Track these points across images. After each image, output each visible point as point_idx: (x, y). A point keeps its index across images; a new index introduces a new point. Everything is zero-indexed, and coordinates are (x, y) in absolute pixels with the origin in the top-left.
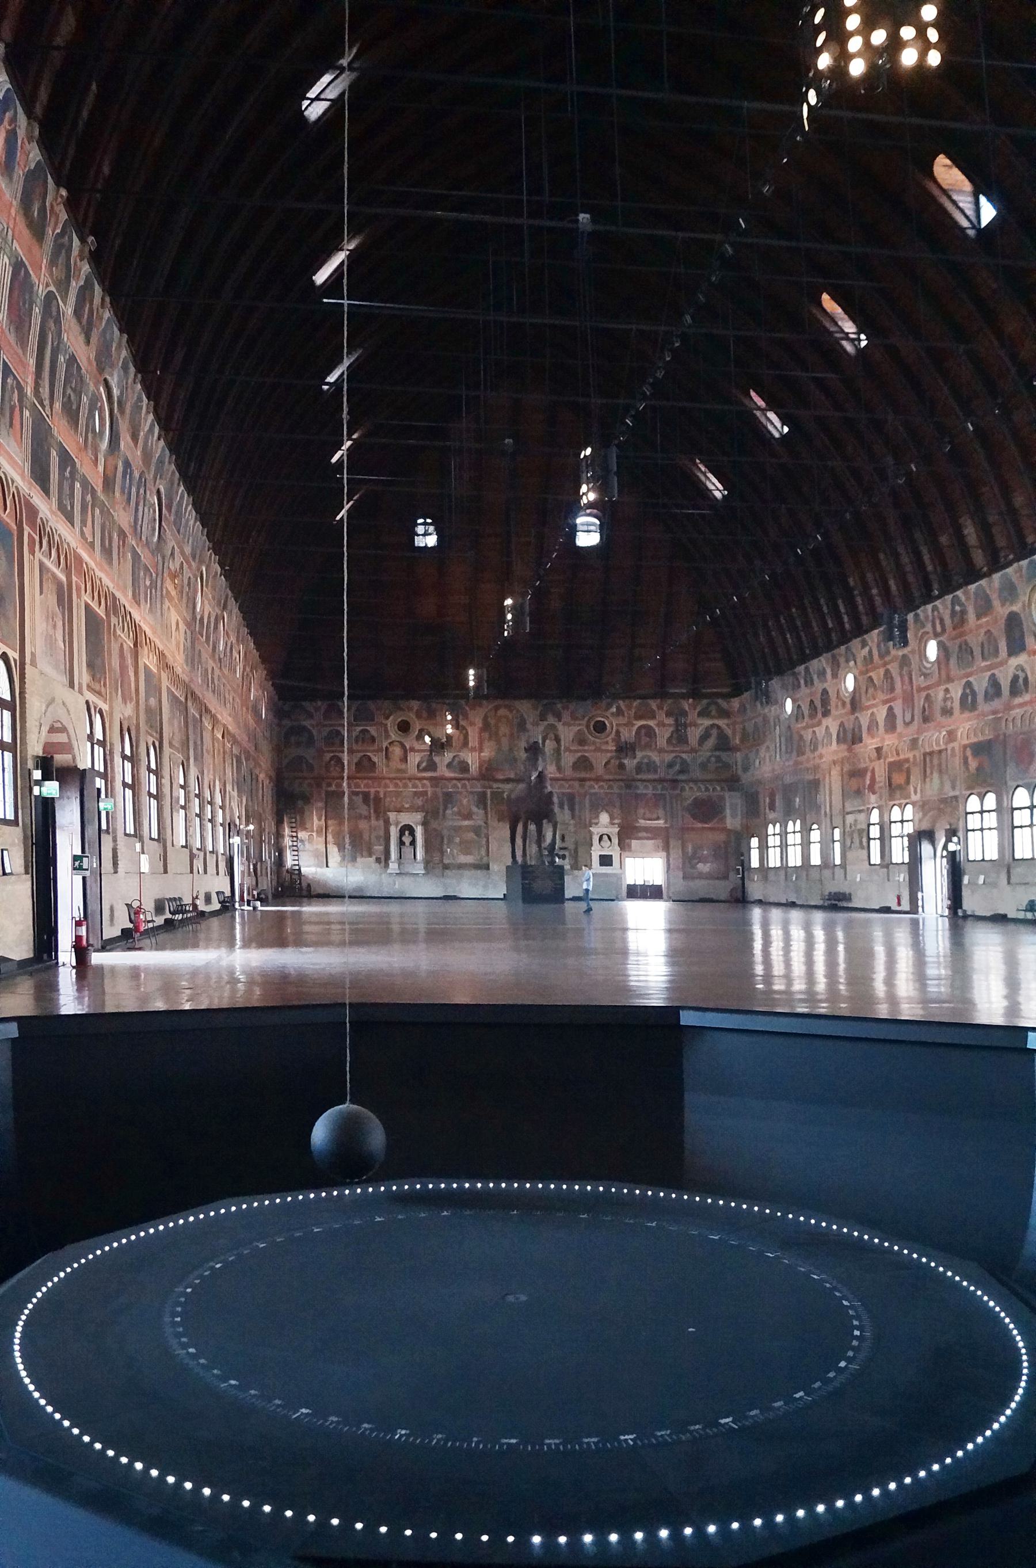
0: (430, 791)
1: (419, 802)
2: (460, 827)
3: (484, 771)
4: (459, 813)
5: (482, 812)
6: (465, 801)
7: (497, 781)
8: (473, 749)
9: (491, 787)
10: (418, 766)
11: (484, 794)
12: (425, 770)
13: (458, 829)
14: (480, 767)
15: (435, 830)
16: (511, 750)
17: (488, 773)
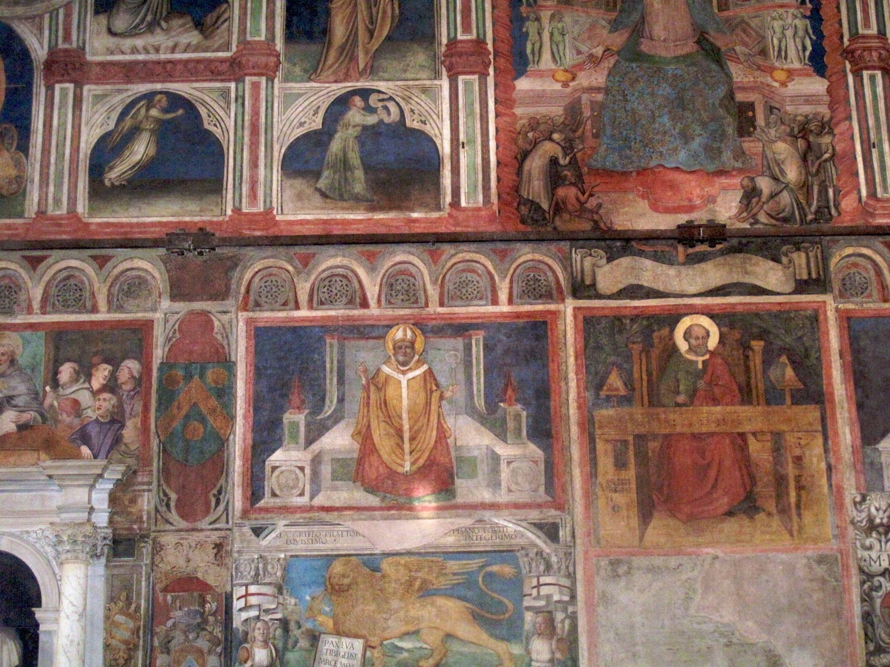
0: (164, 314)
1: (85, 396)
2: (371, 563)
3: (536, 187)
4: (361, 469)
5: (518, 455)
6: (404, 385)
7: (624, 243)
8: (460, 60)
9: (582, 288)
10: (97, 170)
11: (539, 330)
12: (147, 183)
13: (350, 580)
14: (516, 159)
15: (189, 585)
16: (710, 52)
17: (555, 201)
